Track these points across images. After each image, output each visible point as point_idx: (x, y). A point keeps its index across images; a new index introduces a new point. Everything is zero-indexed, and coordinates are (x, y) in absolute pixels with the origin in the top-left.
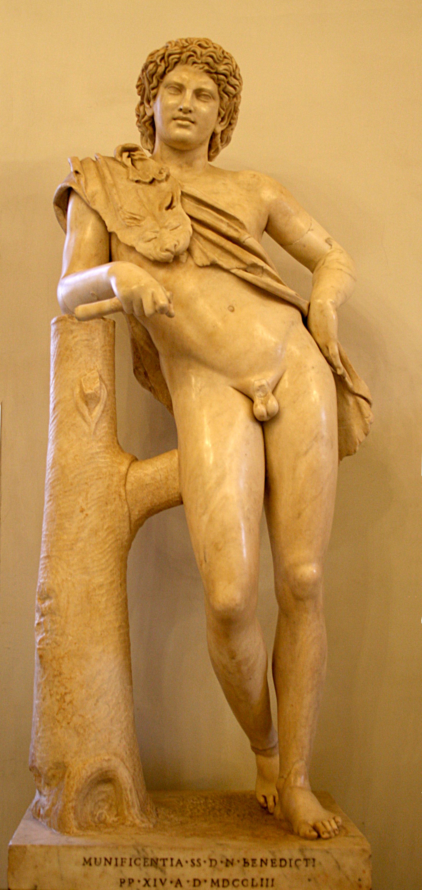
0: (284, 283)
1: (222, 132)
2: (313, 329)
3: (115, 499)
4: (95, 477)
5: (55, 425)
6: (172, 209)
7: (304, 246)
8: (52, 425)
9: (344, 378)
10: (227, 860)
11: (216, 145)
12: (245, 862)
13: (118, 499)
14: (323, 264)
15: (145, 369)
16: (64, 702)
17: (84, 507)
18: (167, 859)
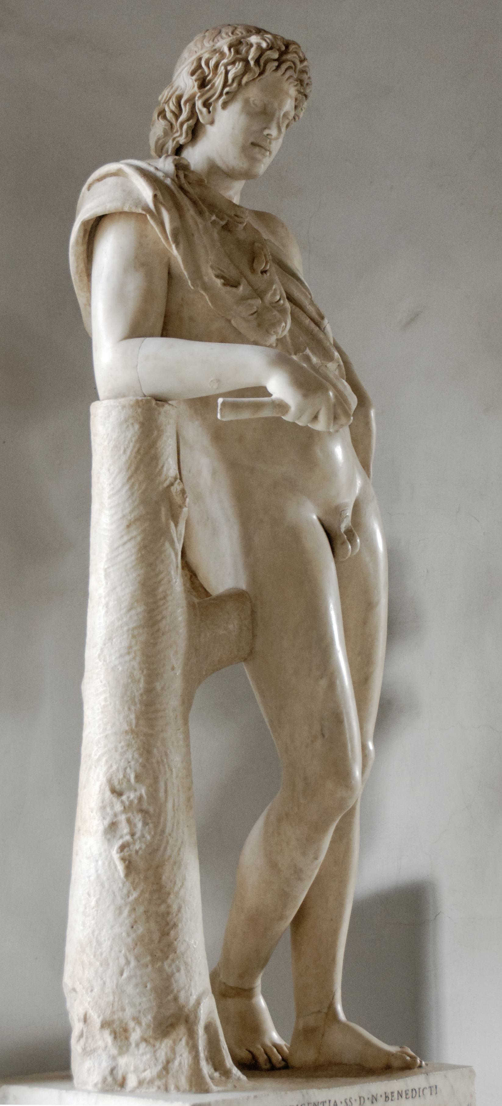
10: (373, 1096)
12: (386, 1097)
16: (167, 924)
18: (326, 1102)
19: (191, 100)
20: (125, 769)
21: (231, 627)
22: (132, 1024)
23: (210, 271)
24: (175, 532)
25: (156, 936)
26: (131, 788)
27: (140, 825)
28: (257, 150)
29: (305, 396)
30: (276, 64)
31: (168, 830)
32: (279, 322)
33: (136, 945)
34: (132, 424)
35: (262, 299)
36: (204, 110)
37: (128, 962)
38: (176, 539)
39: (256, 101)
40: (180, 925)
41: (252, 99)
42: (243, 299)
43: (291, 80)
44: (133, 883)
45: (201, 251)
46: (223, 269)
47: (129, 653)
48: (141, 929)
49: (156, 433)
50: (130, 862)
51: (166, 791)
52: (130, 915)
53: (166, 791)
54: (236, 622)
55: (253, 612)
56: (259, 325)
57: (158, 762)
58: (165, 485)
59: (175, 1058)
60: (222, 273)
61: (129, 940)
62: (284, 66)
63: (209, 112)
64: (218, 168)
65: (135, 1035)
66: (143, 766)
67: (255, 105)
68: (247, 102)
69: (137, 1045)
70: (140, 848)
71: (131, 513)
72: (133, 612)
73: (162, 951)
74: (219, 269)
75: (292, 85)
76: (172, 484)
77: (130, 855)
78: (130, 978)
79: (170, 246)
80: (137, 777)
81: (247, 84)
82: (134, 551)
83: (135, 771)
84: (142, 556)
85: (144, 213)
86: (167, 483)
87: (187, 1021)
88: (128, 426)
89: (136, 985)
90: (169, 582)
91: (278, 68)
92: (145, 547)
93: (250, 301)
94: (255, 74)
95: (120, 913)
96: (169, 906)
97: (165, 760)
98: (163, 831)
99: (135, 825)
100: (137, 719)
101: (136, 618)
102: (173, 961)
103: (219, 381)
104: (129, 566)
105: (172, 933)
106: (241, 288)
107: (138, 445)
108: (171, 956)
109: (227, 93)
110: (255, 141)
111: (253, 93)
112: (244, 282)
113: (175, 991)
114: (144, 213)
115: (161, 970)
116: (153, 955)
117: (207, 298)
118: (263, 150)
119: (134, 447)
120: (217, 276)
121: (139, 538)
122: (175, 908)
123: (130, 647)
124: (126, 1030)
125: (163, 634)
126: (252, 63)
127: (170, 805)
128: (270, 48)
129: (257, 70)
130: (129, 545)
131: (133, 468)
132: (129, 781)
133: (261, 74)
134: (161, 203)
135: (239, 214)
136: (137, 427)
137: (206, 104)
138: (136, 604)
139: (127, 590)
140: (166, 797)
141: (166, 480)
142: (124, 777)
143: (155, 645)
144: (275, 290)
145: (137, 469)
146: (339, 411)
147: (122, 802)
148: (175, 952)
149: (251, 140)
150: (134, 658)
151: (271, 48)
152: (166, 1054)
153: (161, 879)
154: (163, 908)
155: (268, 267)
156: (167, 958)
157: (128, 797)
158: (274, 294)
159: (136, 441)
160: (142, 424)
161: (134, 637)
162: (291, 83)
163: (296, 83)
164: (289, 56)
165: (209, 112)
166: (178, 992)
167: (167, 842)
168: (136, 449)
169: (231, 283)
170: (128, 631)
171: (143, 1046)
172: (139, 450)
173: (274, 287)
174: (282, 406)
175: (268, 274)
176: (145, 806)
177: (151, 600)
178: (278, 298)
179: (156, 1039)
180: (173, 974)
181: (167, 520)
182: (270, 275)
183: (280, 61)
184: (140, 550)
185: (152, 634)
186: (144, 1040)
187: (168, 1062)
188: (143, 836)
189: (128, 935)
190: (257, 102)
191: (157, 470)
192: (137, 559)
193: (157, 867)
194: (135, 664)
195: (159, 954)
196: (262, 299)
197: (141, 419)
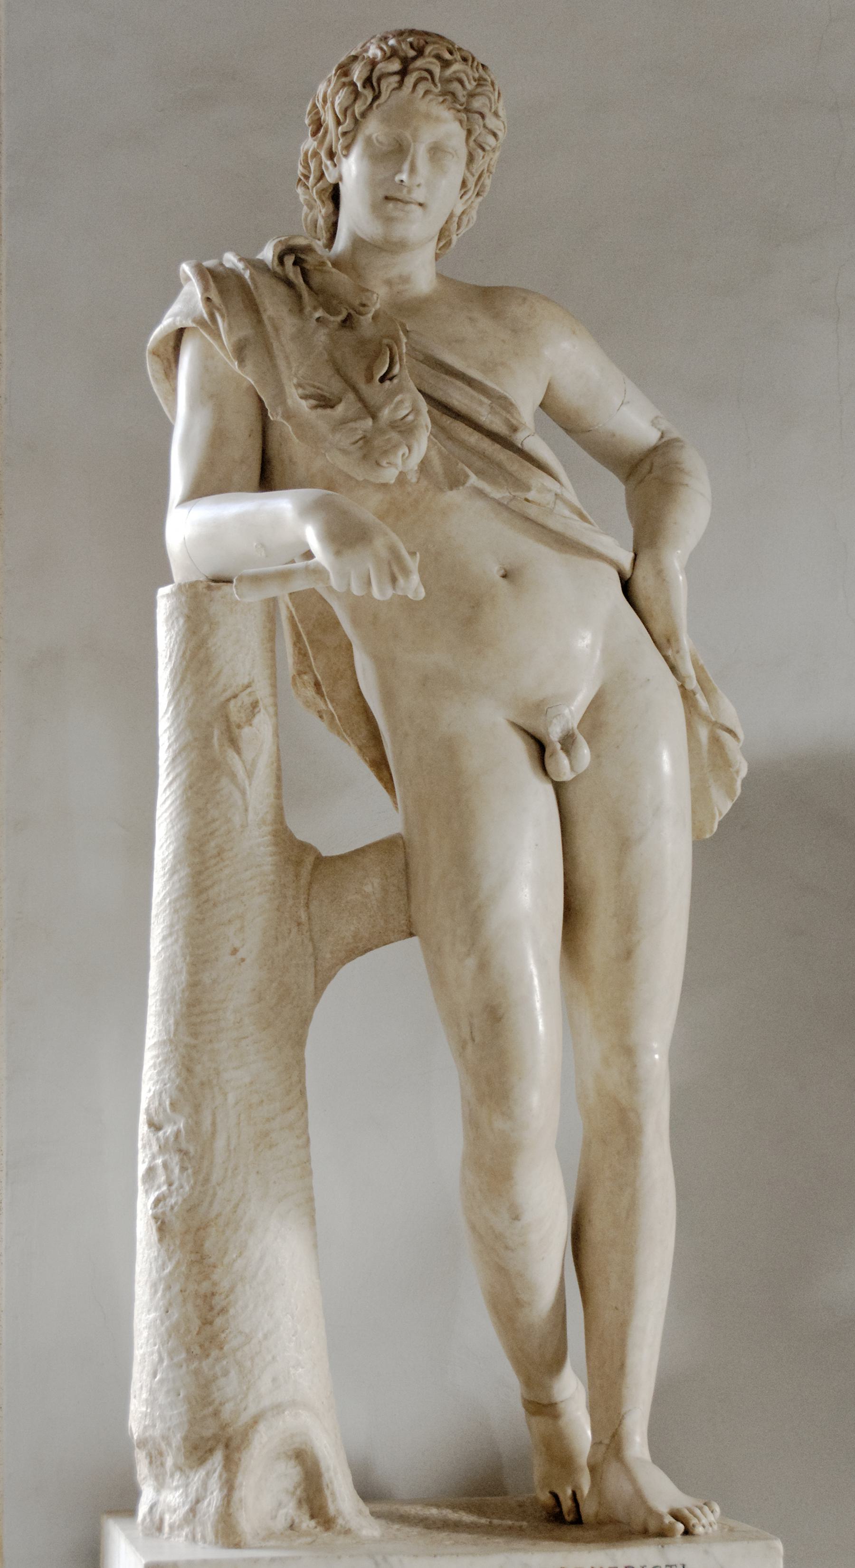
0: (592, 521)
1: (463, 213)
2: (642, 603)
3: (290, 930)
4: (258, 890)
5: (175, 791)
6: (391, 379)
7: (614, 435)
8: (168, 793)
9: (694, 694)
11: (449, 236)
13: (294, 930)
14: (650, 472)
15: (315, 676)
16: (211, 1309)
17: (237, 944)
19: (316, 154)
20: (161, 1094)
21: (368, 889)
22: (163, 1446)
23: (294, 390)
24: (240, 763)
25: (197, 1322)
26: (170, 1121)
27: (177, 1171)
28: (391, 205)
29: (338, 553)
30: (396, 78)
31: (215, 1178)
32: (396, 447)
33: (170, 1336)
34: (177, 618)
35: (374, 417)
36: (329, 163)
37: (161, 1360)
38: (241, 773)
39: (380, 139)
40: (232, 1311)
41: (374, 136)
42: (344, 422)
43: (430, 97)
44: (167, 1250)
45: (281, 363)
46: (316, 384)
47: (171, 934)
48: (175, 1315)
49: (206, 628)
50: (163, 1223)
51: (214, 1124)
52: (164, 1295)
53: (214, 1124)
54: (376, 881)
55: (407, 865)
56: (365, 457)
57: (202, 1084)
58: (222, 699)
59: (204, 1498)
60: (319, 391)
61: (163, 1329)
62: (410, 80)
63: (335, 165)
64: (362, 241)
65: (169, 1462)
66: (181, 1090)
67: (381, 143)
68: (369, 141)
69: (172, 1476)
70: (176, 1203)
71: (176, 740)
72: (176, 877)
73: (201, 1346)
74: (314, 386)
75: (434, 103)
76: (235, 696)
77: (164, 1213)
78: (162, 1381)
79: (233, 364)
80: (171, 1104)
81: (364, 115)
82: (179, 793)
83: (171, 1097)
84: (188, 799)
85: (194, 325)
86: (228, 694)
87: (227, 1446)
88: (173, 622)
89: (168, 1392)
90: (229, 832)
91: (401, 83)
92: (191, 787)
93: (352, 425)
94: (366, 98)
95: (156, 1292)
96: (214, 1284)
97: (215, 1082)
98: (207, 1180)
99: (172, 1171)
100: (177, 1024)
101: (177, 886)
102: (217, 1360)
103: (263, 545)
104: (174, 815)
105: (219, 1321)
106: (340, 409)
107: (183, 647)
108: (215, 1353)
109: (344, 134)
110: (388, 195)
111: (373, 127)
112: (351, 396)
113: (217, 1402)
114: (194, 325)
115: (197, 1373)
116: (188, 1351)
117: (290, 429)
118: (400, 205)
119: (179, 650)
120: (305, 397)
121: (184, 776)
122: (225, 1285)
123: (172, 926)
124: (161, 1454)
125: (215, 905)
126: (359, 85)
127: (220, 1143)
128: (387, 58)
129: (369, 95)
130: (174, 786)
131: (178, 679)
132: (165, 1110)
133: (376, 98)
134: (218, 310)
135: (365, 302)
136: (181, 621)
137: (331, 155)
138: (179, 867)
139: (172, 848)
140: (214, 1134)
141: (224, 691)
142: (160, 1104)
143: (202, 921)
144: (402, 401)
145: (182, 680)
146: (395, 569)
147: (158, 1139)
148: (222, 1348)
149: (381, 193)
150: (176, 941)
151: (387, 58)
152: (197, 1490)
153: (202, 1245)
154: (205, 1286)
155: (396, 370)
156: (208, 1356)
157: (165, 1133)
158: (396, 408)
159: (181, 643)
160: (188, 618)
161: (176, 911)
162: (431, 100)
163: (441, 99)
164: (419, 63)
165: (335, 165)
166: (222, 1404)
167: (215, 1194)
168: (181, 653)
169: (325, 402)
170: (170, 903)
171: (177, 1476)
172: (184, 653)
173: (398, 398)
174: (318, 572)
175: (395, 381)
176: (184, 1145)
177: (197, 860)
178: (406, 412)
179: (191, 1468)
180: (215, 1378)
181: (221, 746)
182: (400, 381)
183: (403, 73)
184: (185, 791)
185: (198, 907)
186: (178, 1468)
187: (198, 1501)
188: (182, 1187)
189: (162, 1323)
190: (382, 138)
191: (210, 678)
192: (181, 804)
193: (198, 1229)
194: (176, 948)
195: (197, 1350)
196: (374, 417)
197: (186, 611)
